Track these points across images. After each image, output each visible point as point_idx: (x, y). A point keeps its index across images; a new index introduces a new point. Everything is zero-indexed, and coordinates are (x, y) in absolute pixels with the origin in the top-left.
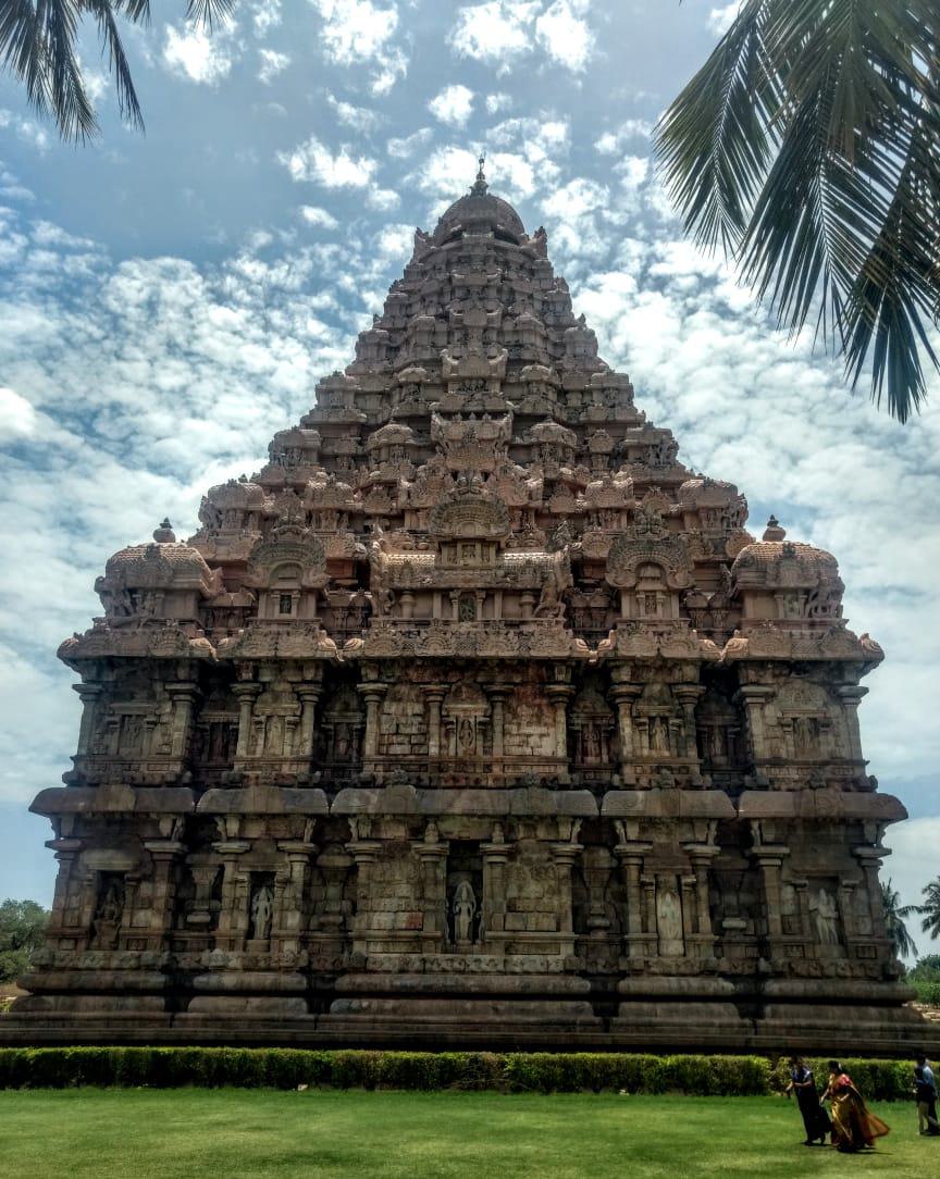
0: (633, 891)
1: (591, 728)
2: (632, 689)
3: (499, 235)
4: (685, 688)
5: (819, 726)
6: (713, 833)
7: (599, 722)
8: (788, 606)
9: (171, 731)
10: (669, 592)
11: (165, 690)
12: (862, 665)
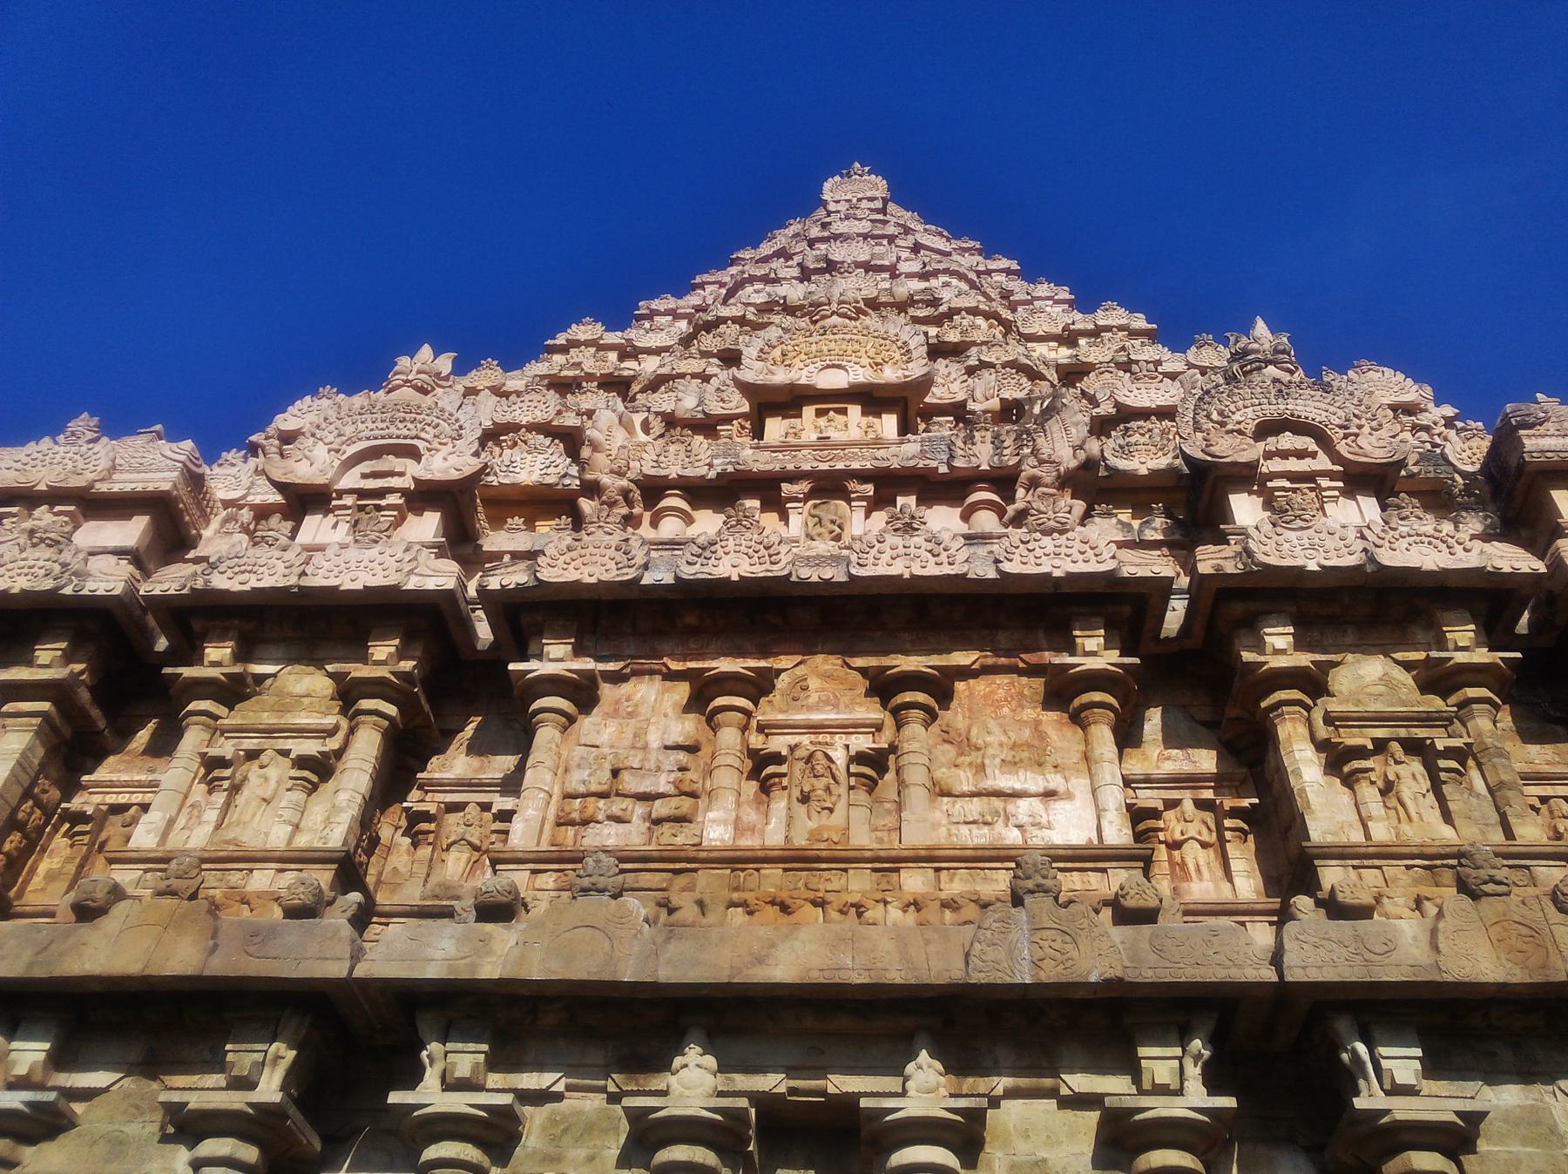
1: (1188, 805)
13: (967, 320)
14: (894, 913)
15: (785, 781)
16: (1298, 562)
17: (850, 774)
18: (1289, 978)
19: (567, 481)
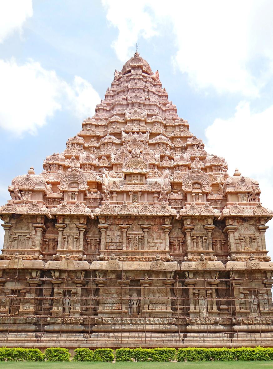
1: (177, 241)
2: (191, 226)
3: (143, 72)
4: (209, 226)
5: (252, 239)
6: (218, 276)
7: (179, 239)
8: (242, 198)
9: (35, 241)
10: (203, 193)
11: (33, 226)
12: (266, 218)
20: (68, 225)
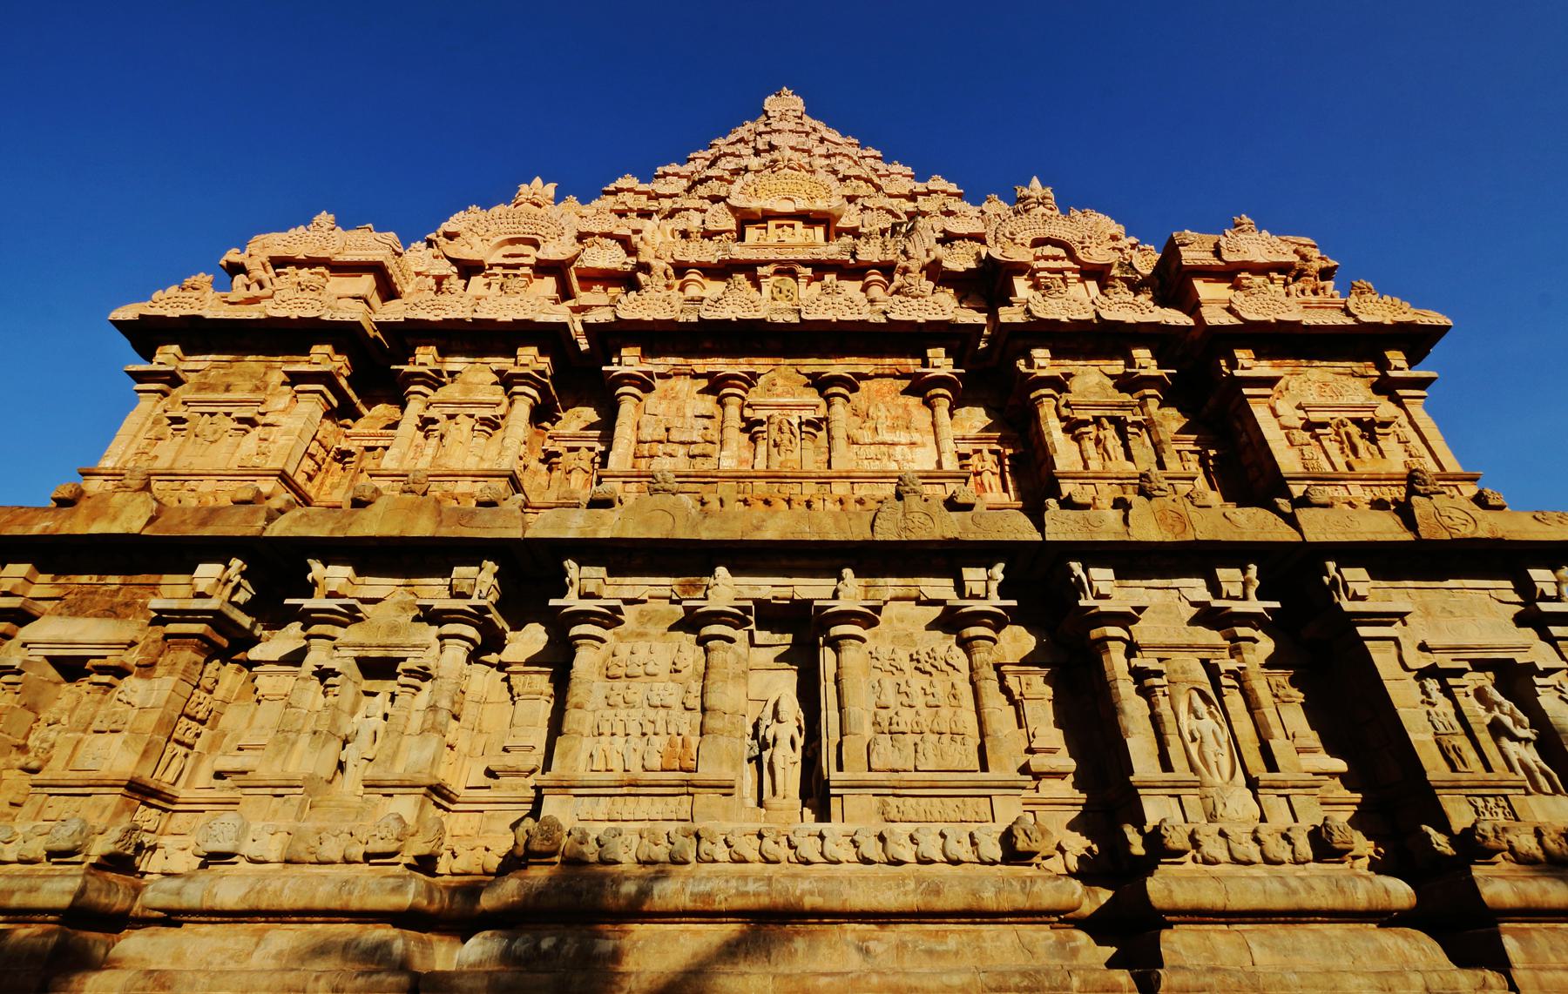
0: (1126, 688)
1: (986, 452)
13: (855, 183)
14: (829, 505)
15: (765, 435)
16: (1056, 317)
17: (801, 432)
18: (1048, 539)
19: (626, 266)
20: (457, 376)
